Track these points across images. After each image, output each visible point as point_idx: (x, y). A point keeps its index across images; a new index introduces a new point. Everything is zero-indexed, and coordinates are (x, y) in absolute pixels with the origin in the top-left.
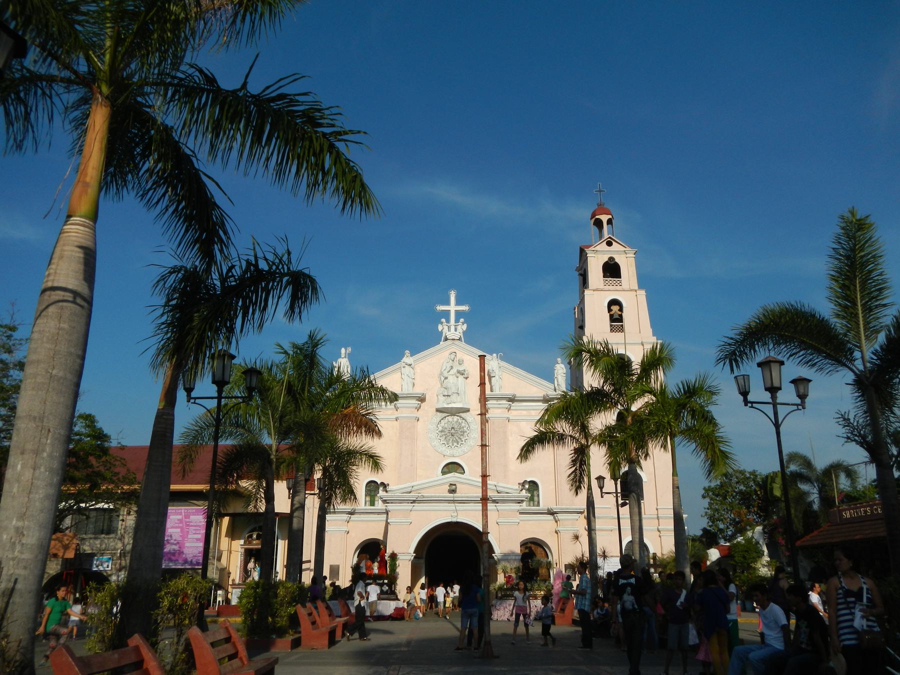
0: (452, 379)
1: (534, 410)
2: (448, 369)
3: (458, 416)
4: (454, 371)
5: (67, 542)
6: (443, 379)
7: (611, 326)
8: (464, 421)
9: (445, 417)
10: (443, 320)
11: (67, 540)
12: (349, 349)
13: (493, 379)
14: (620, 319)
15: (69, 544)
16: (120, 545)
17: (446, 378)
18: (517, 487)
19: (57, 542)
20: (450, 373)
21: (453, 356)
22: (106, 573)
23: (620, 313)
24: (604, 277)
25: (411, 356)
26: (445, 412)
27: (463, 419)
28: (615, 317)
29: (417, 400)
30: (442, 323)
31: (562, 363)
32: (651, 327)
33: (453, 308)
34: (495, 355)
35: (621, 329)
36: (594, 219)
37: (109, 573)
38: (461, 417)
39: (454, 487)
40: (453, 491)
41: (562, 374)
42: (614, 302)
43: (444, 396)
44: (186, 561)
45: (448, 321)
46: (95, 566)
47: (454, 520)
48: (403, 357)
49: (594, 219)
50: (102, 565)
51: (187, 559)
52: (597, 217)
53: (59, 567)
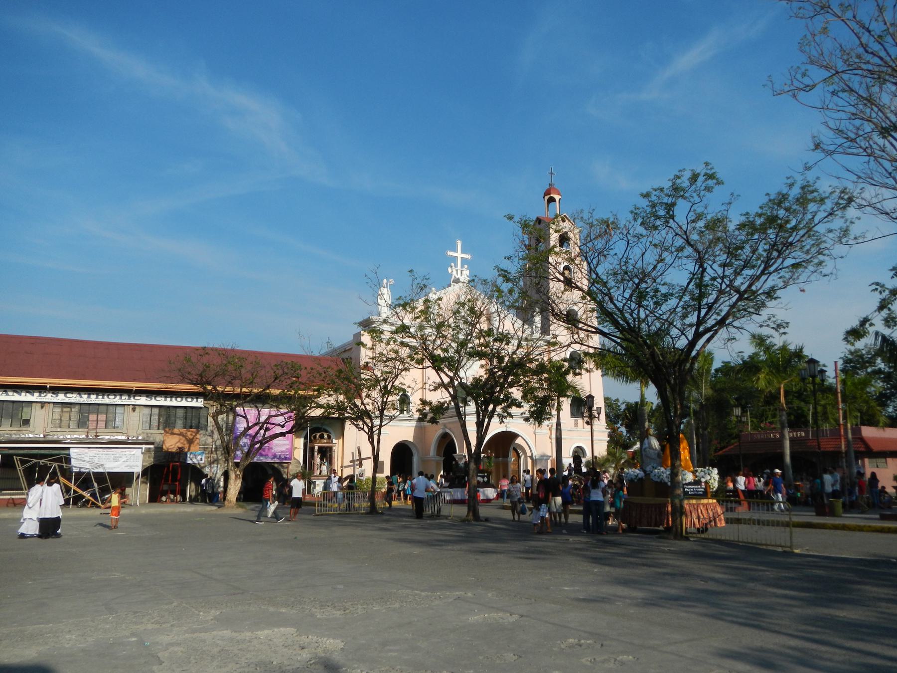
5: (191, 437)
10: (453, 264)
11: (191, 435)
12: (392, 281)
15: (193, 438)
16: (210, 440)
19: (181, 437)
22: (200, 465)
30: (451, 267)
33: (459, 255)
36: (549, 196)
37: (202, 465)
44: (275, 456)
45: (456, 266)
46: (188, 459)
49: (549, 196)
50: (196, 458)
51: (275, 454)
52: (552, 195)
53: (152, 460)
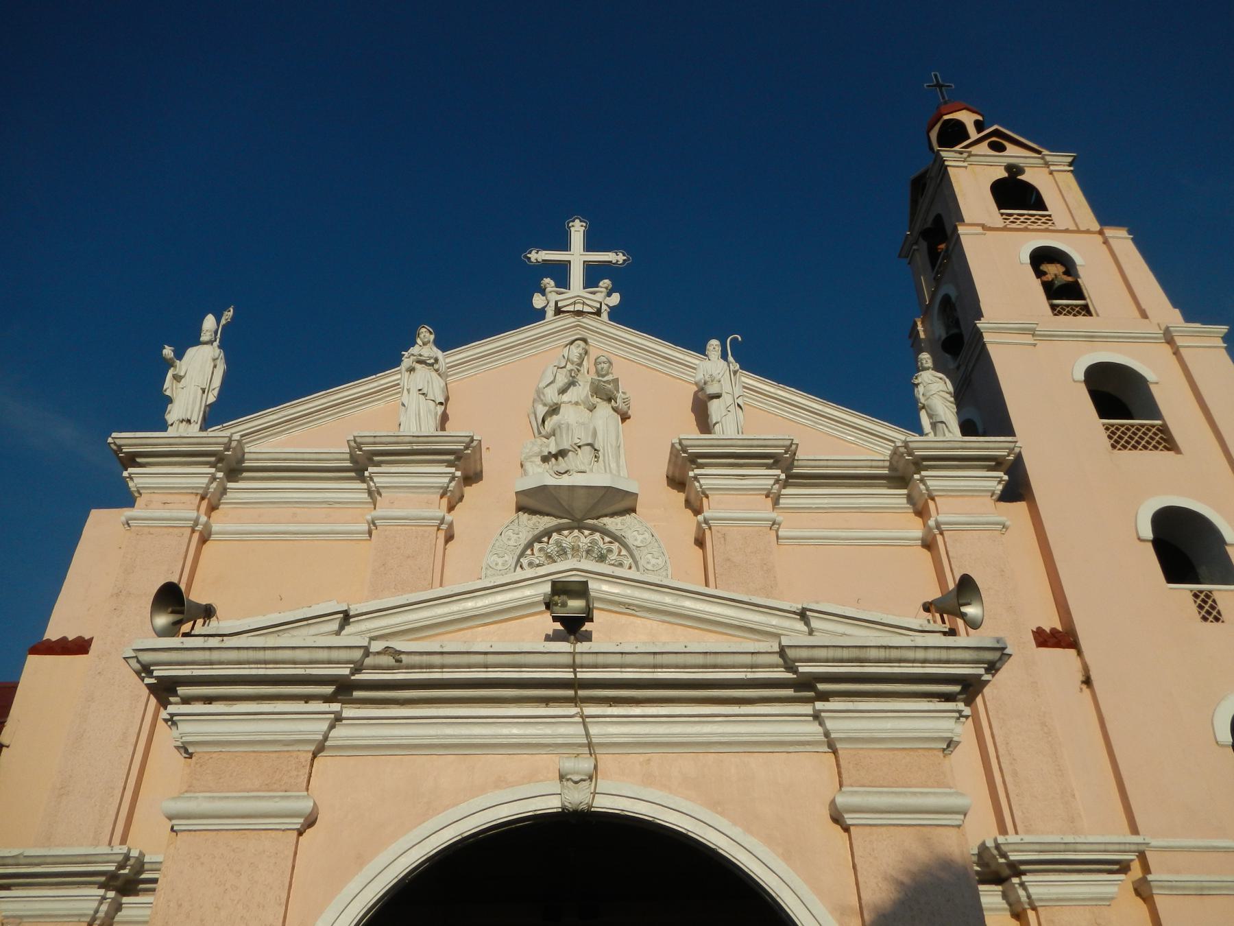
0: (568, 415)
1: (860, 509)
2: (562, 380)
3: (594, 529)
4: (581, 391)
6: (541, 410)
7: (1053, 307)
8: (615, 546)
9: (548, 533)
10: (548, 282)
12: (228, 315)
13: (715, 407)
14: (1074, 290)
17: (554, 410)
18: (920, 620)
20: (565, 398)
21: (575, 351)
23: (1070, 279)
24: (999, 209)
25: (444, 343)
26: (548, 515)
27: (615, 538)
28: (1057, 283)
29: (450, 464)
31: (937, 368)
32: (1175, 303)
33: (577, 256)
34: (714, 344)
35: (1086, 310)
38: (605, 532)
39: (576, 604)
40: (573, 627)
41: (948, 396)
42: (1041, 258)
43: (545, 459)
47: (577, 798)
48: (414, 343)
52: (946, 117)
